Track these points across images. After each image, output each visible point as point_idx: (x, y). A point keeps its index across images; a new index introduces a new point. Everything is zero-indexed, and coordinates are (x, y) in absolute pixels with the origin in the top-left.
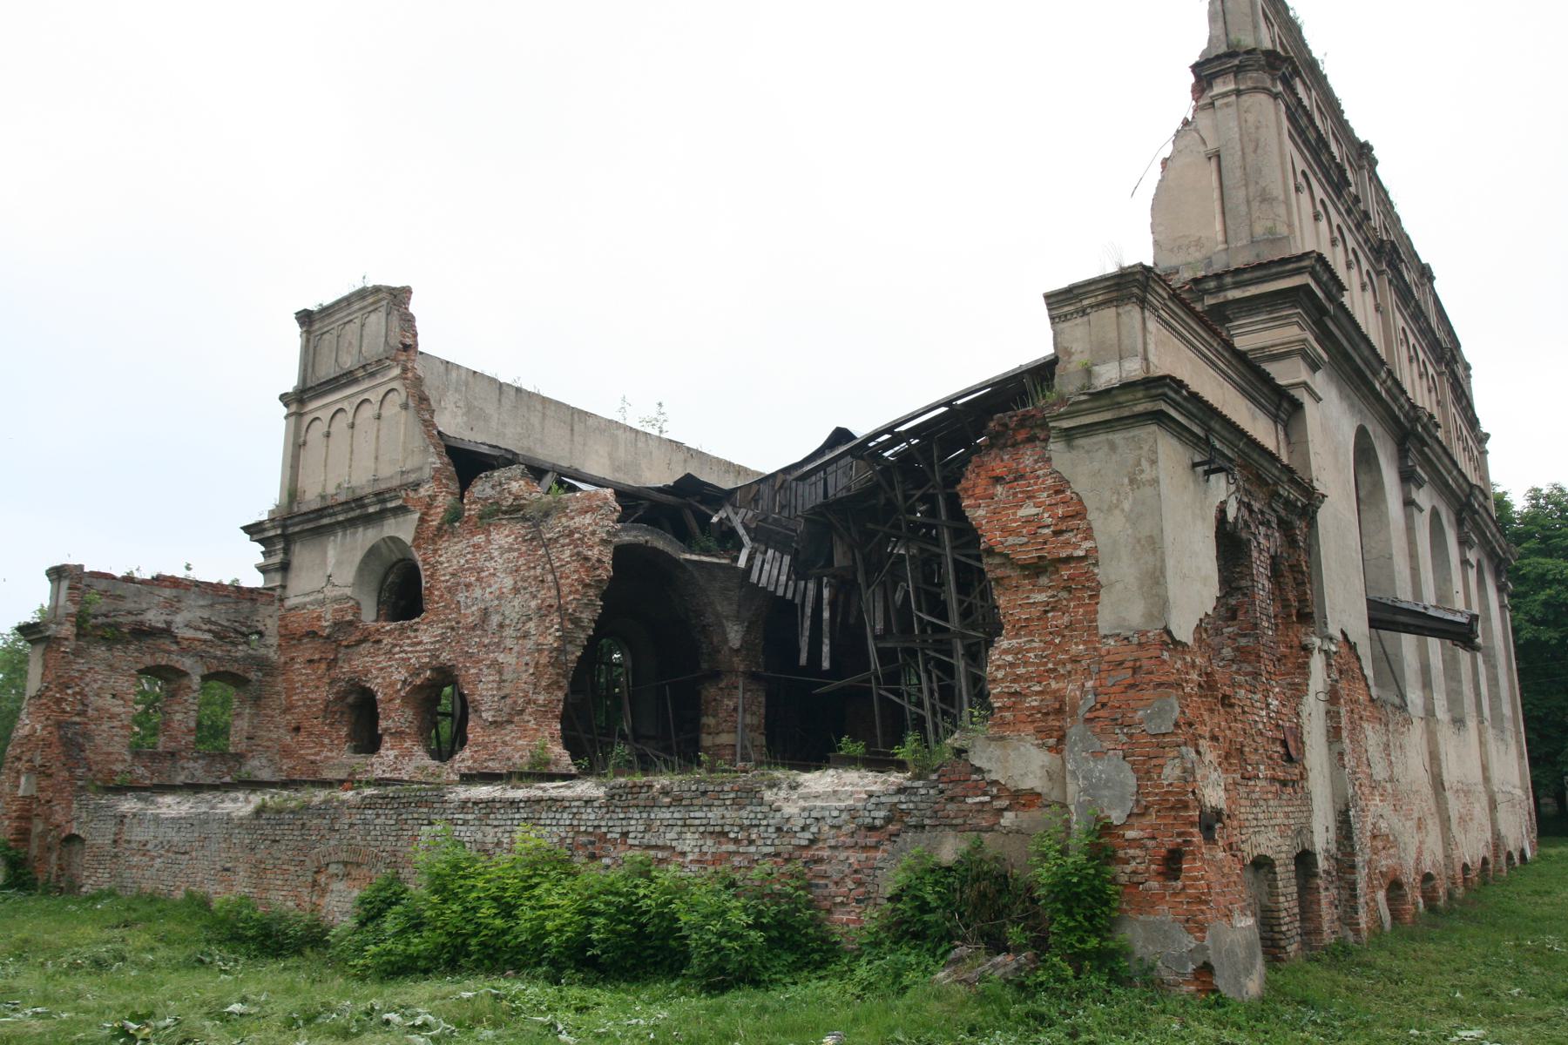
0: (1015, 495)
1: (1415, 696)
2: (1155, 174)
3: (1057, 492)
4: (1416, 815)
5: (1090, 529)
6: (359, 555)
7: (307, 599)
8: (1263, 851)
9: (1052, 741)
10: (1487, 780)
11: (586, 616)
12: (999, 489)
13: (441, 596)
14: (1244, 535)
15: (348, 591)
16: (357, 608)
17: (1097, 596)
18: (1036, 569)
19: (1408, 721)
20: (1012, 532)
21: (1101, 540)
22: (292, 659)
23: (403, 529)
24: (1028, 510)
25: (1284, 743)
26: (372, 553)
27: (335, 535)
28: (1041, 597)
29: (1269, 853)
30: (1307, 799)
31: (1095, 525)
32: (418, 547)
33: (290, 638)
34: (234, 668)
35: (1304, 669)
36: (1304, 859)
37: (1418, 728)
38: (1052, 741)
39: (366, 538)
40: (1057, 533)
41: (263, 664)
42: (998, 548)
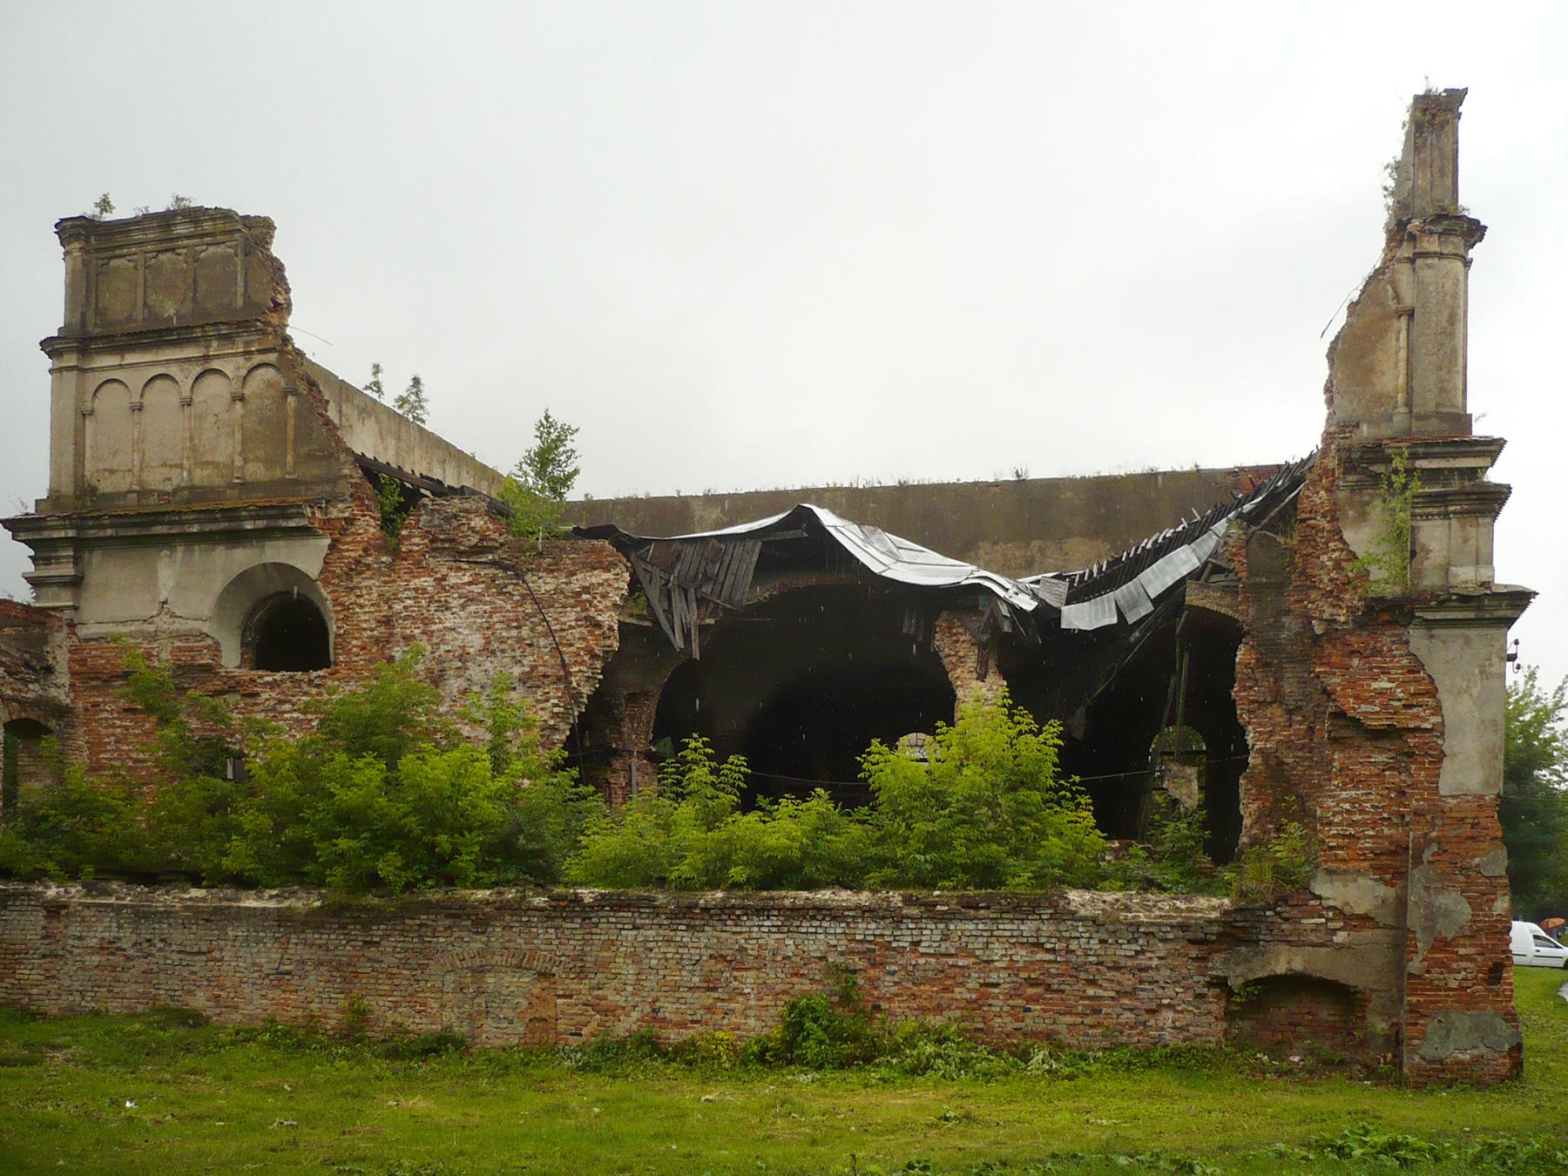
0: (1371, 669)
3: (1410, 672)
6: (219, 584)
7: (122, 629)
11: (586, 690)
12: (1355, 662)
13: (363, 648)
15: (205, 628)
16: (216, 649)
17: (1440, 761)
18: (1378, 735)
20: (1366, 701)
22: (96, 705)
23: (308, 558)
26: (243, 579)
27: (172, 549)
31: (1446, 705)
32: (327, 583)
33: (89, 675)
34: (33, 715)
39: (243, 558)
40: (1406, 707)
41: (62, 712)
42: (1350, 713)
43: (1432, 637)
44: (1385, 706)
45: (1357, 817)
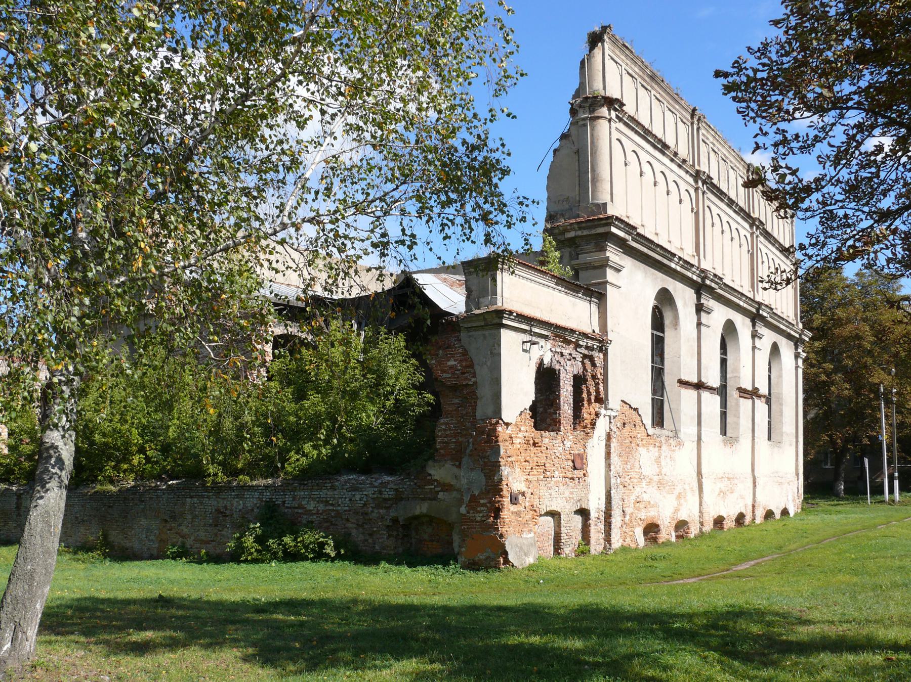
1: (688, 430)
2: (550, 158)
4: (676, 492)
5: (474, 373)
8: (554, 508)
9: (457, 463)
10: (753, 470)
14: (557, 367)
19: (680, 444)
21: (479, 378)
24: (452, 363)
25: (573, 461)
28: (457, 401)
29: (558, 509)
30: (587, 487)
35: (593, 425)
36: (583, 513)
37: (690, 447)
38: (457, 463)
43: (470, 336)
44: (453, 374)
45: (448, 433)
